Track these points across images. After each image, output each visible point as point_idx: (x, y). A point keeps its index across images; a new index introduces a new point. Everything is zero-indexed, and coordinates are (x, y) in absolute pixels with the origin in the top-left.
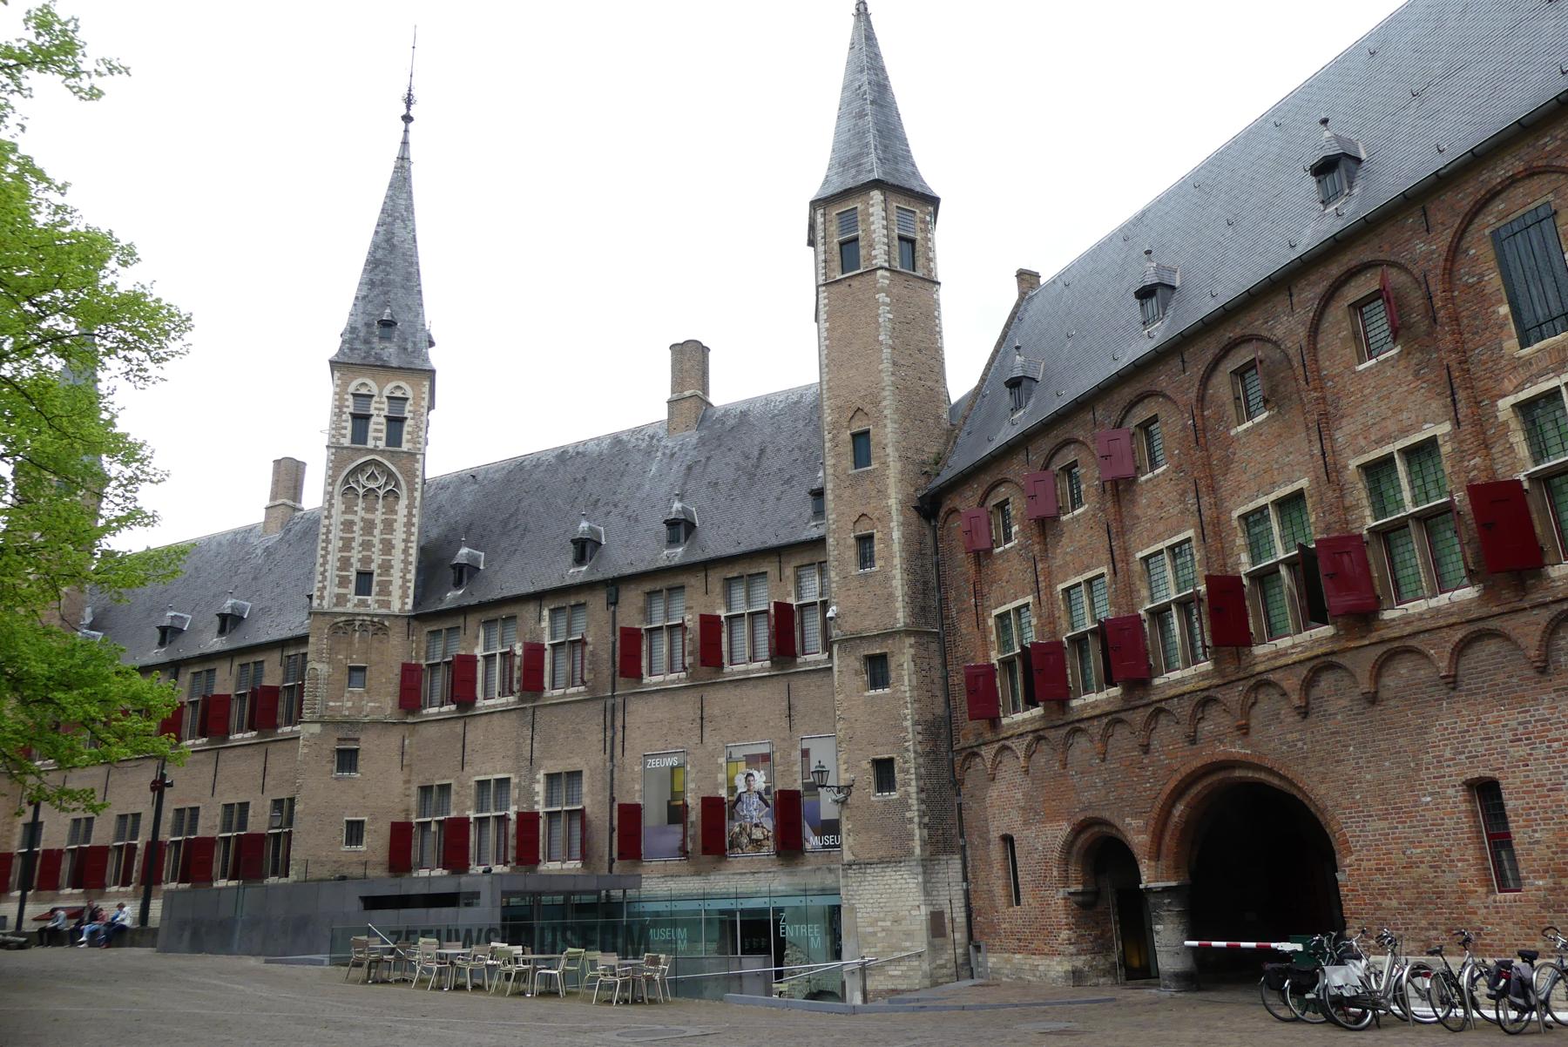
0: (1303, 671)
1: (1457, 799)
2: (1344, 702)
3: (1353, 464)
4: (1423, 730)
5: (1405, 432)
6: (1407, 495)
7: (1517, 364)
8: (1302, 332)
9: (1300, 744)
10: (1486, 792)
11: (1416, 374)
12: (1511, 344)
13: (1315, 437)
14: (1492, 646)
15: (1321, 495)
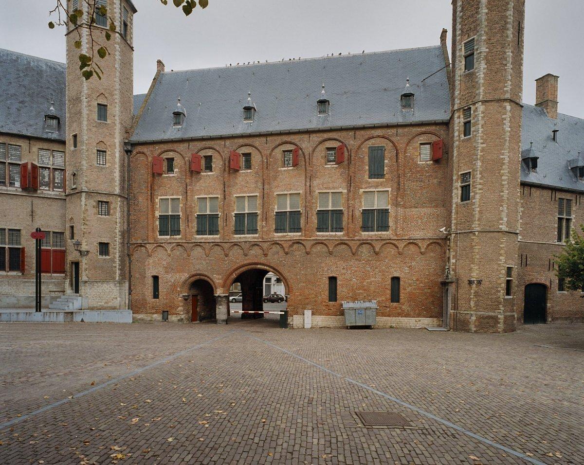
0: (291, 243)
1: (327, 281)
2: (300, 253)
3: (317, 191)
4: (320, 263)
5: (334, 188)
6: (330, 204)
7: (367, 182)
8: (311, 149)
9: (283, 262)
10: (333, 280)
11: (341, 175)
12: (367, 177)
13: (308, 180)
14: (344, 246)
15: (306, 196)
